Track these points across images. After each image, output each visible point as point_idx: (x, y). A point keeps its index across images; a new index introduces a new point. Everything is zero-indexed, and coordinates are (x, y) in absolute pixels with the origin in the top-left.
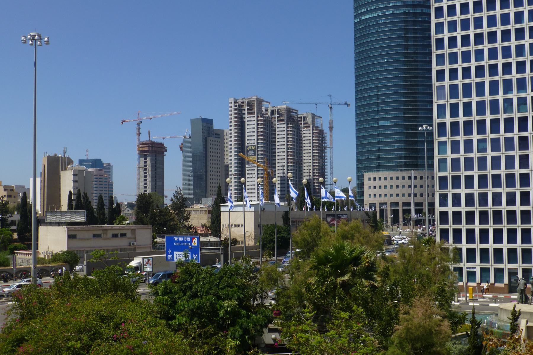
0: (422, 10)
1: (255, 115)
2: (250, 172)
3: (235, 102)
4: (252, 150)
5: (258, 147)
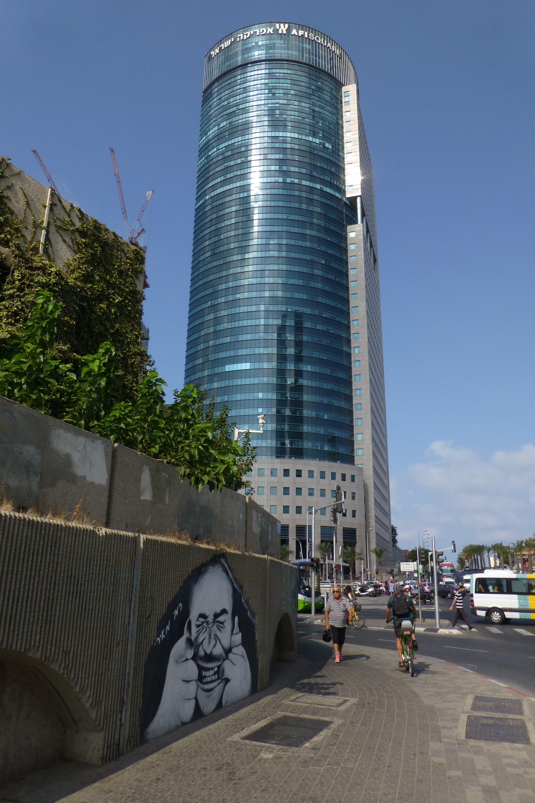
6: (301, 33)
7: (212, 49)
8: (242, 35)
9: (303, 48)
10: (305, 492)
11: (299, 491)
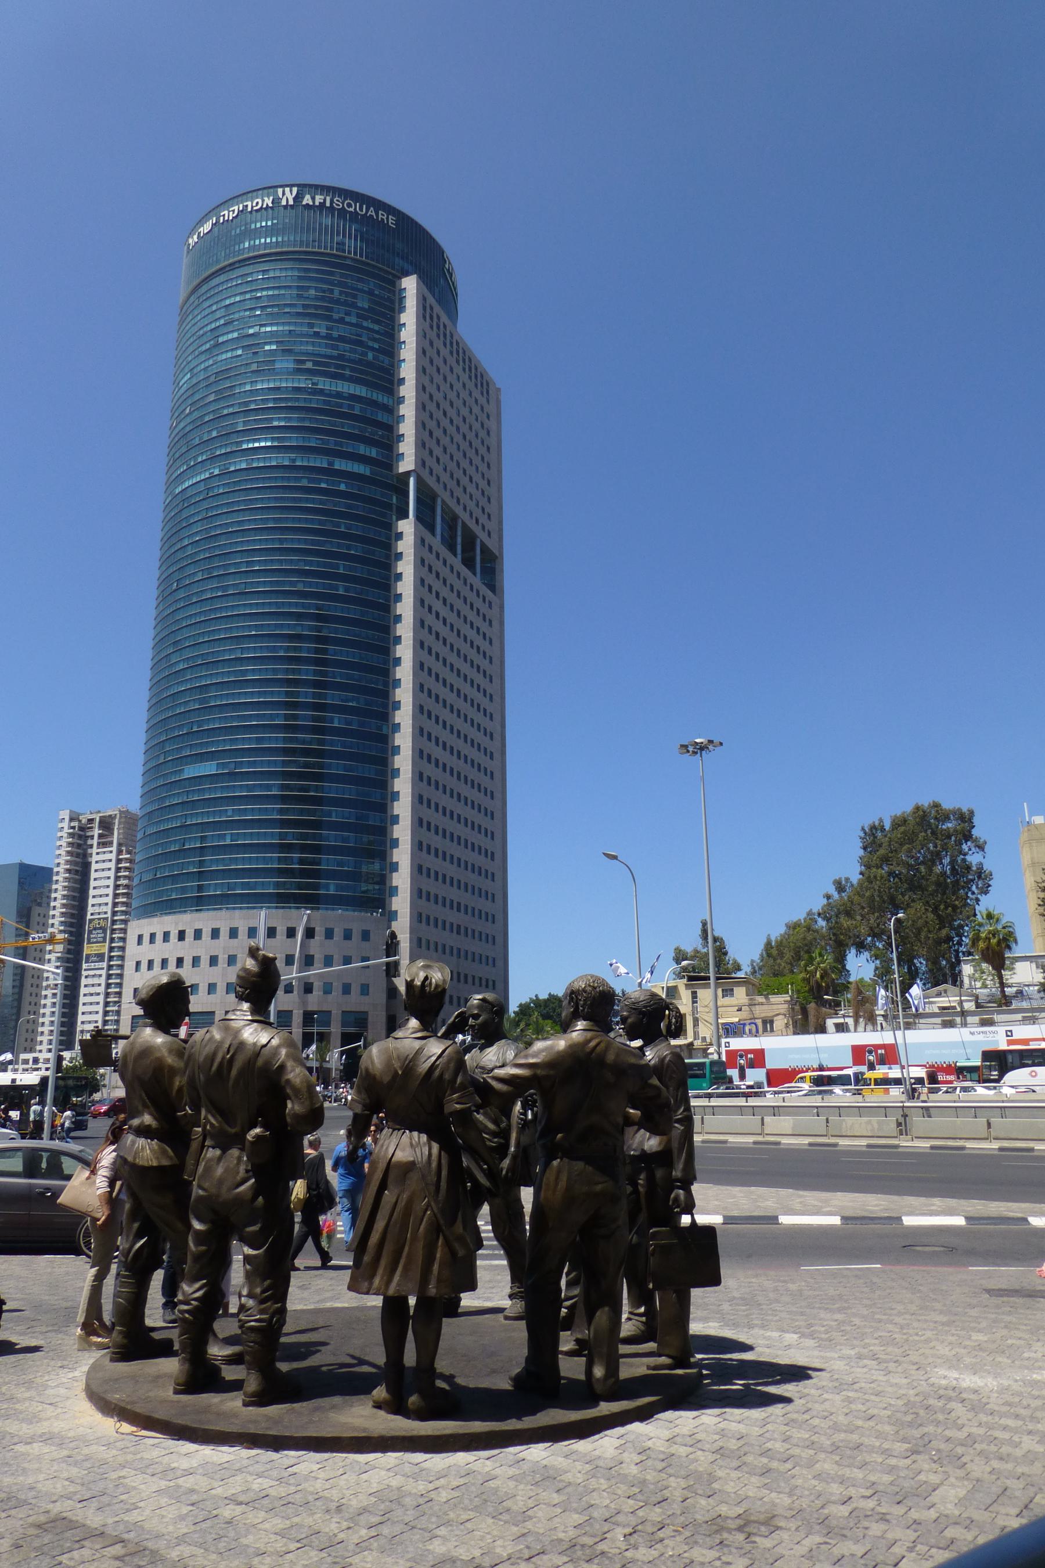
0: (331, 463)
1: (114, 848)
2: (90, 981)
3: (71, 820)
4: (100, 928)
5: (114, 922)
6: (319, 199)
7: (190, 235)
8: (226, 212)
9: (321, 224)
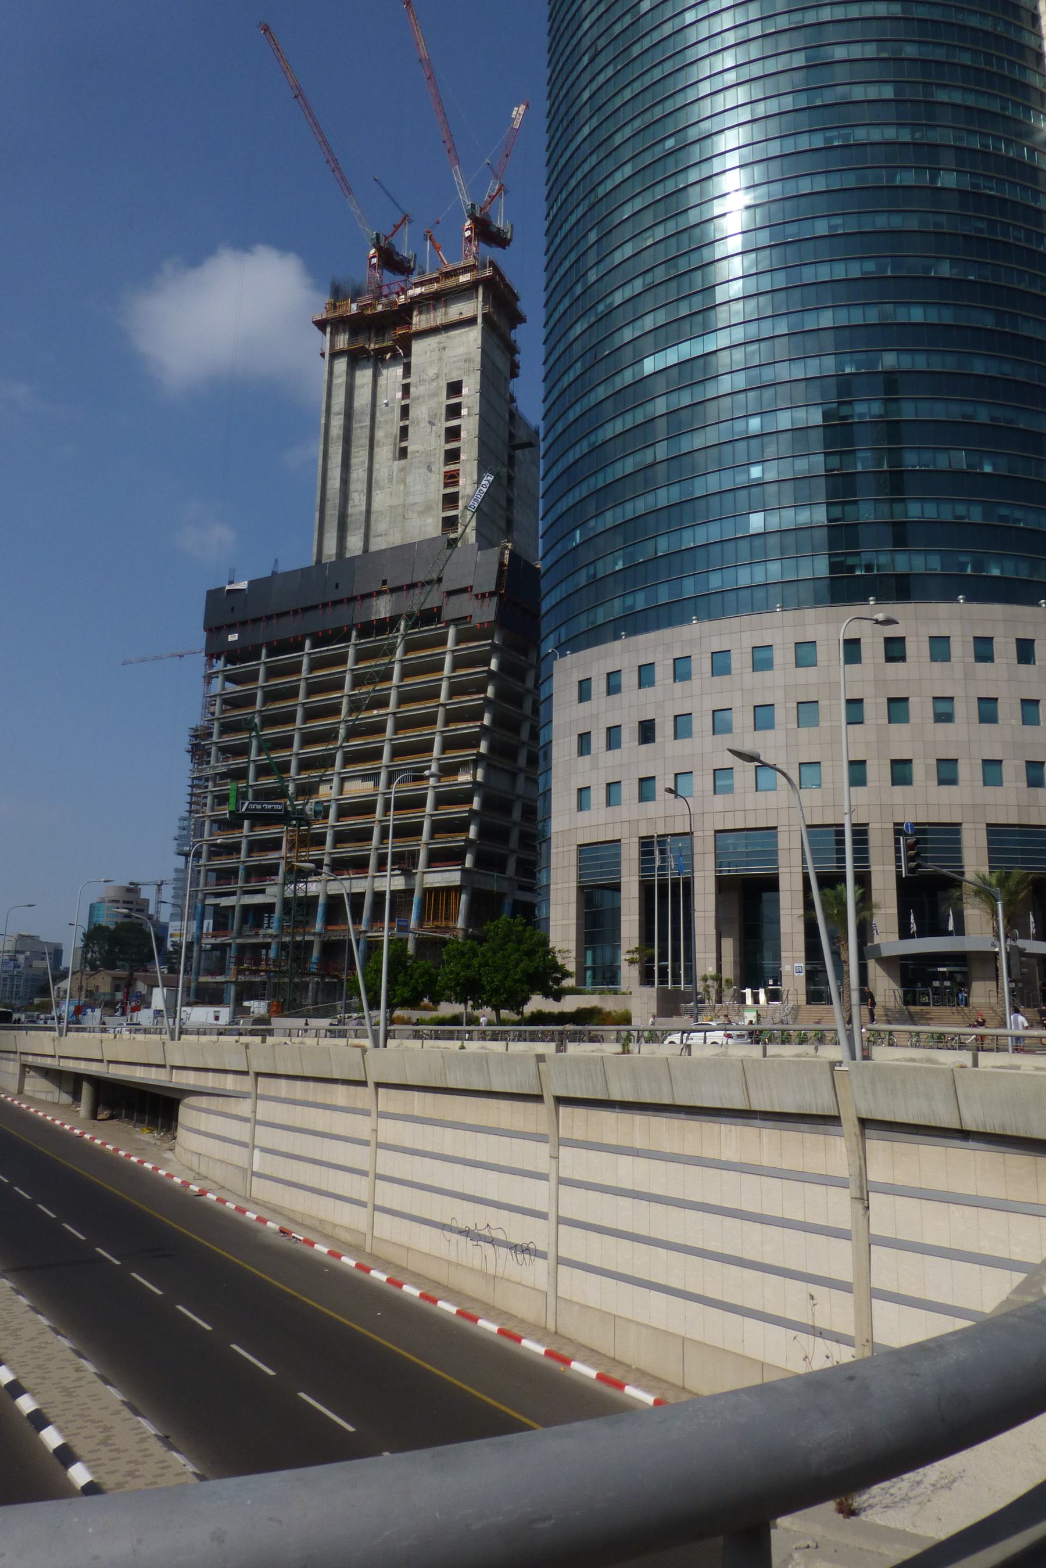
10: (921, 709)
11: (897, 708)
